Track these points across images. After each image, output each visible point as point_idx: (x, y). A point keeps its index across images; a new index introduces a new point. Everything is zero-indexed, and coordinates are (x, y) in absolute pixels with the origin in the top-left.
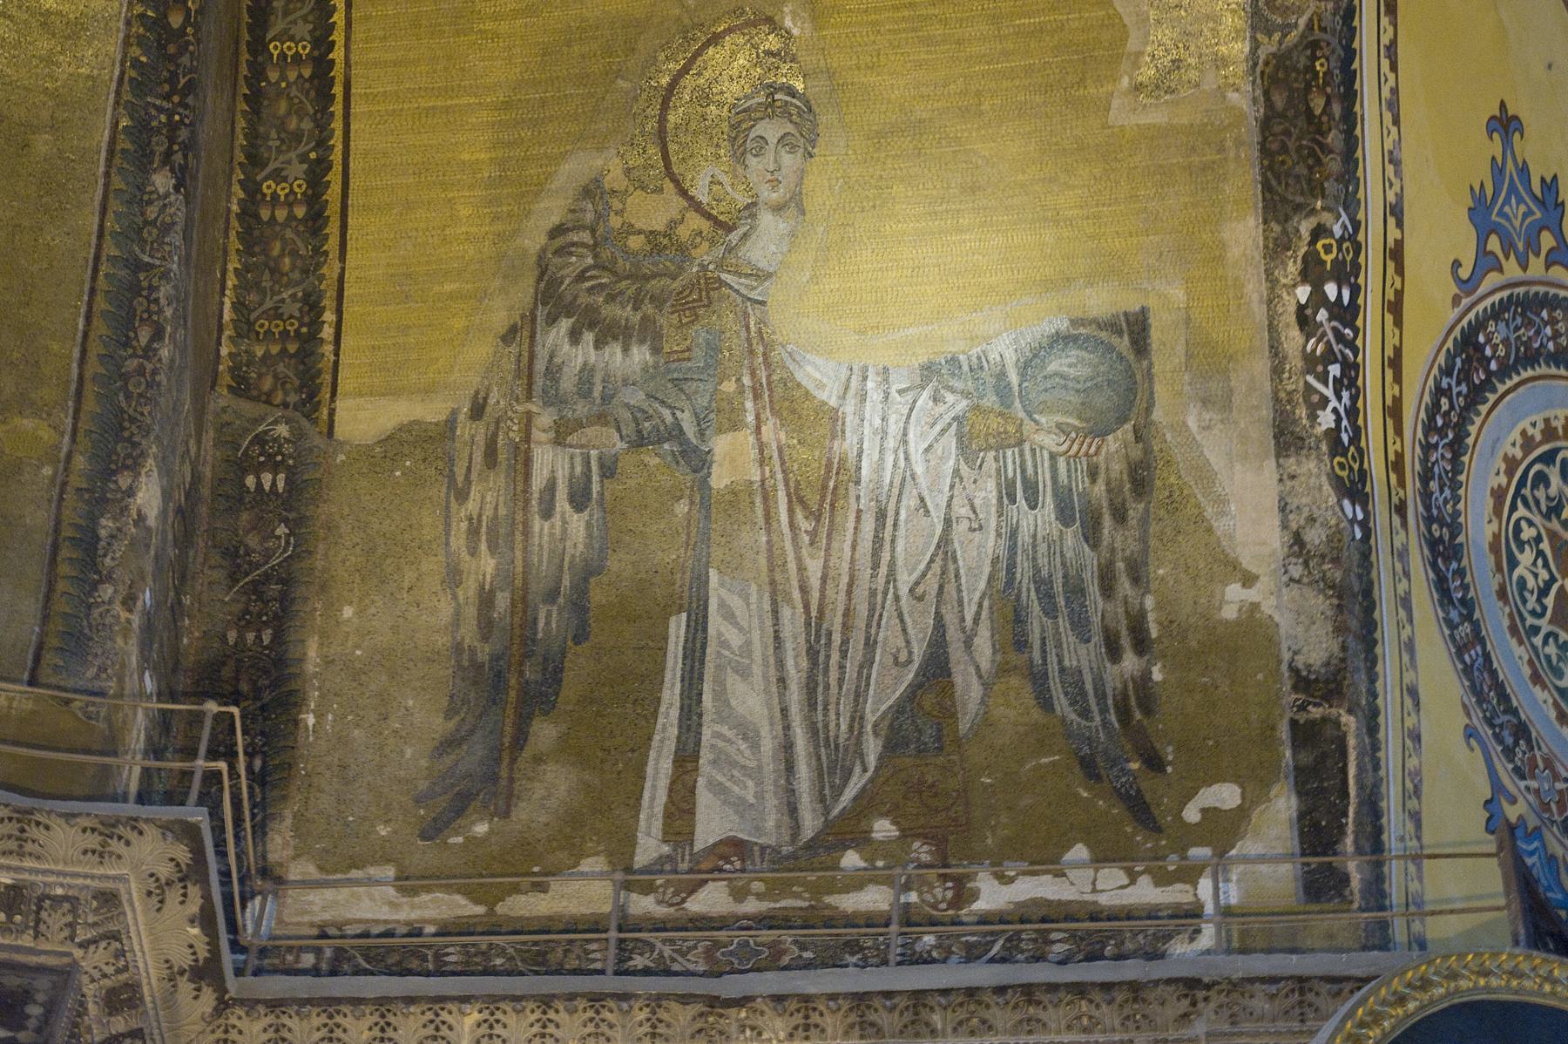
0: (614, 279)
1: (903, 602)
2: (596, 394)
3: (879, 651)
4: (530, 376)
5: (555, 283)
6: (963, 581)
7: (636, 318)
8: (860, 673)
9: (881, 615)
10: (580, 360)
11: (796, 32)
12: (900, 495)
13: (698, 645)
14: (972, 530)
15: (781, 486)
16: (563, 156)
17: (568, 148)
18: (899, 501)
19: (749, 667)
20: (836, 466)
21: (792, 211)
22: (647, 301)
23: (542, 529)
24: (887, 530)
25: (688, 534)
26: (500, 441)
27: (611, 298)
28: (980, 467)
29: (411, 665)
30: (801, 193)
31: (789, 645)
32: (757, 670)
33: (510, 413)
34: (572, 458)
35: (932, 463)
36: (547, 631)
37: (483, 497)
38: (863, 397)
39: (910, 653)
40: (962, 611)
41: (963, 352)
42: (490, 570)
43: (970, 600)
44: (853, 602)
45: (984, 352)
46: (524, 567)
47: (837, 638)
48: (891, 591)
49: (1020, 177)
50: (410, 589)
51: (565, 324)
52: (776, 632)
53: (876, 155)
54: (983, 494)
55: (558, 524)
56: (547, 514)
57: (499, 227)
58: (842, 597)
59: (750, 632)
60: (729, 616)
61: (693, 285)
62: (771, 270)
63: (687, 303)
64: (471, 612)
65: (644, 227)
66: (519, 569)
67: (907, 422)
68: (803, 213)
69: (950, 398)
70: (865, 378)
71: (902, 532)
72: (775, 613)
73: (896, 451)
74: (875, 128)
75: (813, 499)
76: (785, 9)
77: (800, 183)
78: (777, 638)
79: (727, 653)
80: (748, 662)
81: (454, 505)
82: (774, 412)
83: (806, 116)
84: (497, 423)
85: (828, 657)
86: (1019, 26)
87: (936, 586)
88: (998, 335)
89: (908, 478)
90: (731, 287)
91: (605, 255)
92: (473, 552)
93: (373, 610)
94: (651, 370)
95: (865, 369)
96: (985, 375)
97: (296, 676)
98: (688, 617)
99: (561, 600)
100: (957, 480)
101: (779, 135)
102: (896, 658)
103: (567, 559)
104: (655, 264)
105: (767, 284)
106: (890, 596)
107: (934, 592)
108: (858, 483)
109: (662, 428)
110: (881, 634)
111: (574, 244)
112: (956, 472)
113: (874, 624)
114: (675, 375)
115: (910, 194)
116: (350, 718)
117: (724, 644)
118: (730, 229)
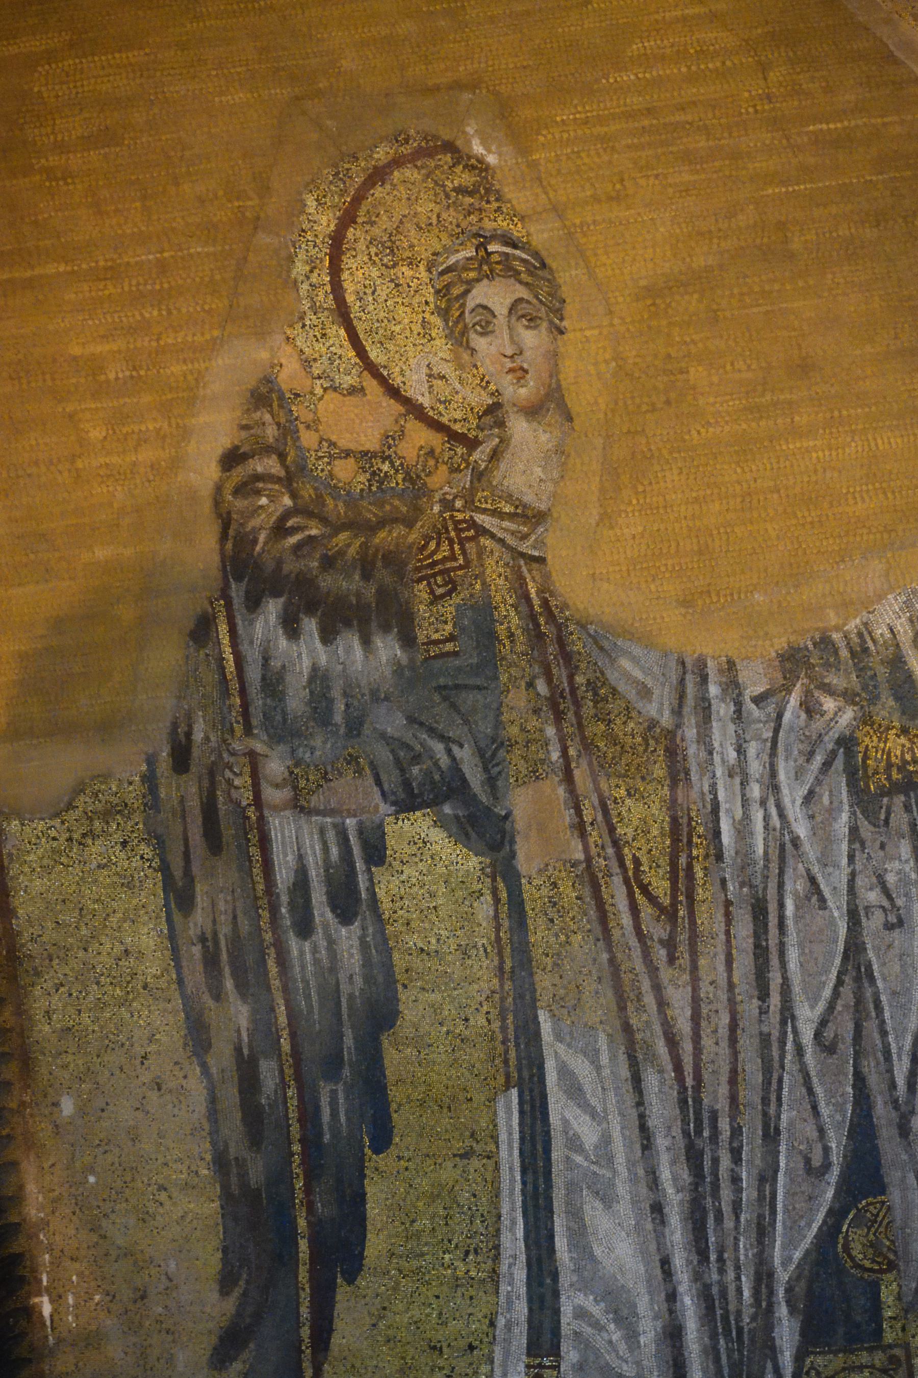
0: (328, 530)
1: (809, 1058)
2: (338, 718)
3: (783, 1148)
4: (243, 692)
5: (245, 541)
6: (887, 1015)
7: (370, 592)
8: (761, 1191)
9: (780, 1081)
10: (306, 663)
11: (491, 159)
12: (781, 873)
13: (540, 1148)
14: (889, 927)
15: (616, 870)
16: (214, 346)
17: (216, 333)
18: (781, 885)
19: (611, 1184)
20: (686, 829)
21: (552, 416)
22: (379, 564)
23: (302, 953)
24: (770, 936)
25: (500, 954)
26: (222, 806)
27: (328, 563)
28: (887, 821)
29: (163, 1196)
30: (559, 387)
31: (661, 1142)
32: (622, 1189)
33: (225, 755)
34: (322, 832)
35: (819, 819)
36: (336, 1133)
37: (213, 905)
38: (705, 710)
39: (826, 1150)
40: (890, 1071)
41: (837, 628)
42: (244, 1023)
43: (900, 1049)
44: (741, 1057)
45: (866, 624)
46: (289, 1016)
47: (724, 1125)
48: (790, 1037)
49: (868, 348)
50: (145, 1057)
51: (273, 608)
52: (642, 1117)
53: (654, 323)
54: (896, 865)
55: (323, 943)
56: (305, 928)
57: (146, 455)
58: (724, 1049)
59: (605, 1118)
60: (574, 1091)
61: (439, 534)
62: (543, 507)
63: (435, 563)
64: (230, 1095)
65: (352, 446)
66: (283, 1020)
67: (773, 753)
68: (570, 419)
69: (829, 704)
70: (704, 679)
71: (792, 938)
72: (637, 1080)
73: (763, 803)
74: (643, 283)
75: (660, 886)
76: (470, 130)
77: (554, 372)
78: (643, 1128)
79: (579, 1159)
80: (609, 1175)
81: (177, 917)
82: (588, 746)
83: (540, 273)
84: (212, 774)
85: (716, 1161)
86: (813, 132)
87: (851, 1026)
88: (880, 597)
89: (789, 846)
90: (493, 536)
91: (307, 492)
92: (218, 995)
93: (99, 1103)
94: (407, 673)
95: (701, 664)
96: (874, 662)
97: (16, 1228)
98: (520, 1096)
99: (346, 1072)
100: (857, 846)
101: (508, 301)
102: (808, 1161)
103: (344, 1001)
104: (380, 504)
105: (541, 529)
106: (789, 1046)
107: (849, 1036)
108: (719, 857)
109: (437, 777)
110: (784, 1117)
111: (258, 478)
112: (854, 832)
113: (773, 1097)
114: (442, 681)
115: (715, 379)
116: (97, 1298)
117: (574, 1143)
118: (473, 444)
